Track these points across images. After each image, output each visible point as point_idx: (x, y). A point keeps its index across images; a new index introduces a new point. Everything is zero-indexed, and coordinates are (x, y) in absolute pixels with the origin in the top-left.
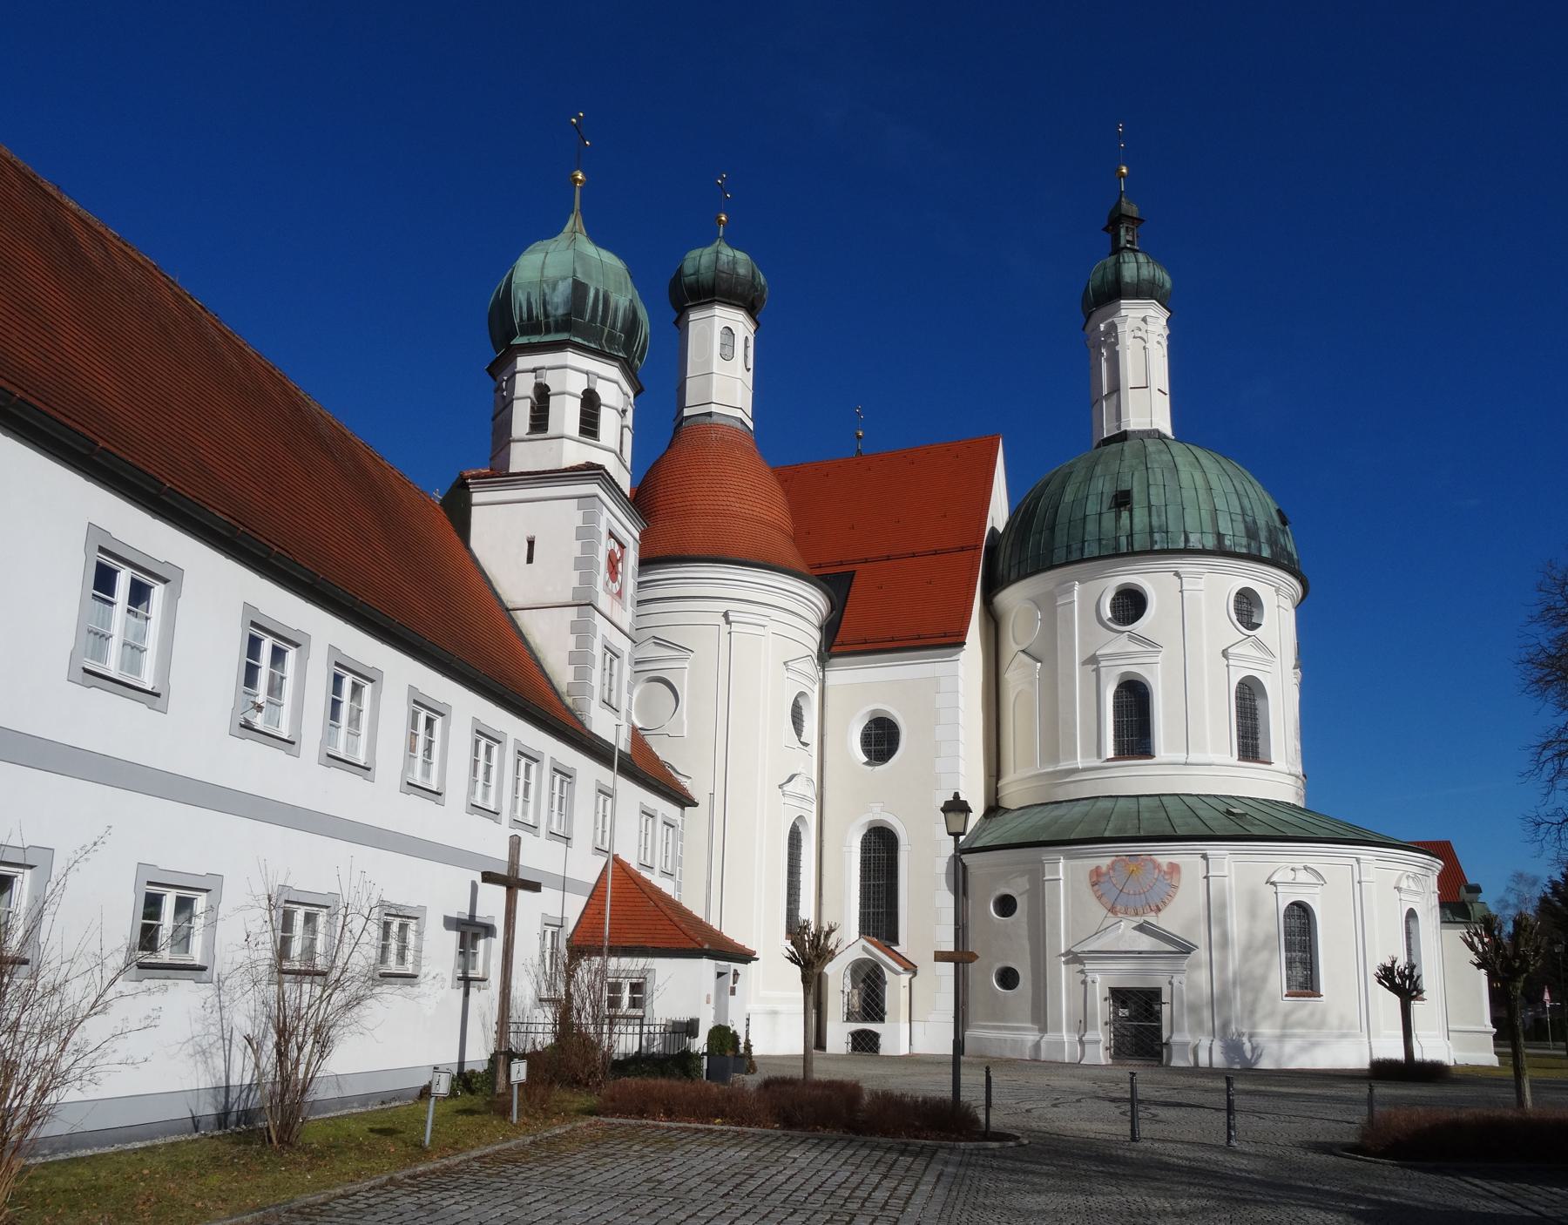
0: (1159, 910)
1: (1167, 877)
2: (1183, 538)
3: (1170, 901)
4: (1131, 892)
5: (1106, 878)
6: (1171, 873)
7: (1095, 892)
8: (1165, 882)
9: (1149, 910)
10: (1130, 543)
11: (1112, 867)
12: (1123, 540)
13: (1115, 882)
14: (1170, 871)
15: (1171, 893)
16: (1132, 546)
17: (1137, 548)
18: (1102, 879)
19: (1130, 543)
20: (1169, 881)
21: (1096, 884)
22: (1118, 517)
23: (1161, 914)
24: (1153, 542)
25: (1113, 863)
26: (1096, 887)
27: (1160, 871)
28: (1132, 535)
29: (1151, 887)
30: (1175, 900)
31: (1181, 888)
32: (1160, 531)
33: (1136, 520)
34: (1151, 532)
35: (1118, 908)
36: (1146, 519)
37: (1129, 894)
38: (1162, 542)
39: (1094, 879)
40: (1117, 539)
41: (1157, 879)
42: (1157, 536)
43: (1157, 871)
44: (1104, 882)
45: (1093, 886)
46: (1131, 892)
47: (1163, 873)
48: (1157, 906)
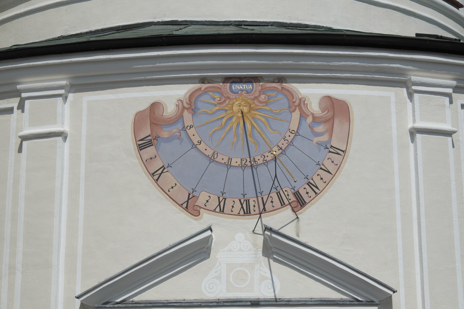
1: (320, 128)
3: (327, 184)
4: (236, 161)
5: (175, 129)
6: (330, 121)
7: (146, 163)
8: (316, 140)
9: (277, 203)
13: (195, 140)
14: (330, 114)
15: (328, 165)
18: (165, 134)
20: (325, 138)
21: (149, 144)
25: (192, 96)
26: (150, 151)
27: (303, 116)
29: (283, 152)
30: (340, 179)
31: (351, 153)
35: (201, 201)
37: (229, 165)
39: (146, 132)
41: (297, 134)
43: (296, 115)
44: (168, 140)
45: (141, 147)
46: (236, 161)
47: (310, 119)
48: (297, 194)
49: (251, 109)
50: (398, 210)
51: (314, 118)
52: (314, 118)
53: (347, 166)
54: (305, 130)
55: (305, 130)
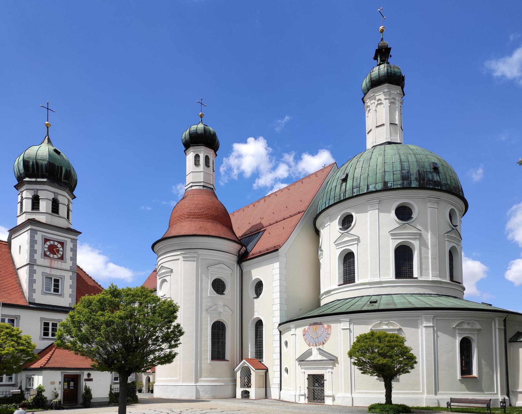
0: (324, 344)
1: (326, 330)
2: (366, 188)
8: (326, 332)
10: (345, 195)
11: (309, 329)
12: (342, 195)
15: (328, 337)
16: (345, 197)
17: (347, 197)
19: (345, 195)
22: (341, 186)
23: (324, 345)
24: (353, 193)
27: (324, 328)
28: (345, 192)
32: (356, 187)
33: (348, 185)
34: (353, 189)
36: (352, 183)
38: (357, 192)
40: (340, 195)
41: (323, 332)
42: (355, 190)
43: (323, 328)
47: (325, 329)
48: (323, 342)
49: (317, 328)
50: (339, 343)
51: (326, 329)
52: (326, 329)
53: (330, 337)
54: (324, 331)
55: (324, 331)
